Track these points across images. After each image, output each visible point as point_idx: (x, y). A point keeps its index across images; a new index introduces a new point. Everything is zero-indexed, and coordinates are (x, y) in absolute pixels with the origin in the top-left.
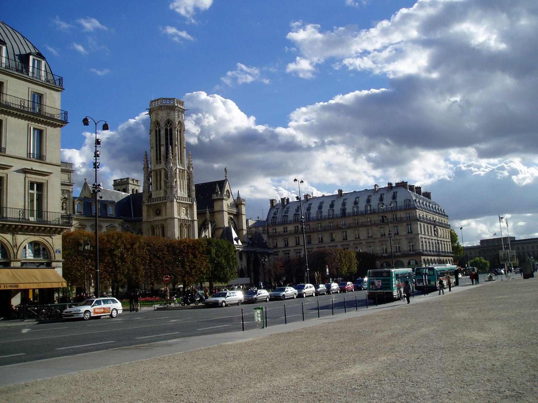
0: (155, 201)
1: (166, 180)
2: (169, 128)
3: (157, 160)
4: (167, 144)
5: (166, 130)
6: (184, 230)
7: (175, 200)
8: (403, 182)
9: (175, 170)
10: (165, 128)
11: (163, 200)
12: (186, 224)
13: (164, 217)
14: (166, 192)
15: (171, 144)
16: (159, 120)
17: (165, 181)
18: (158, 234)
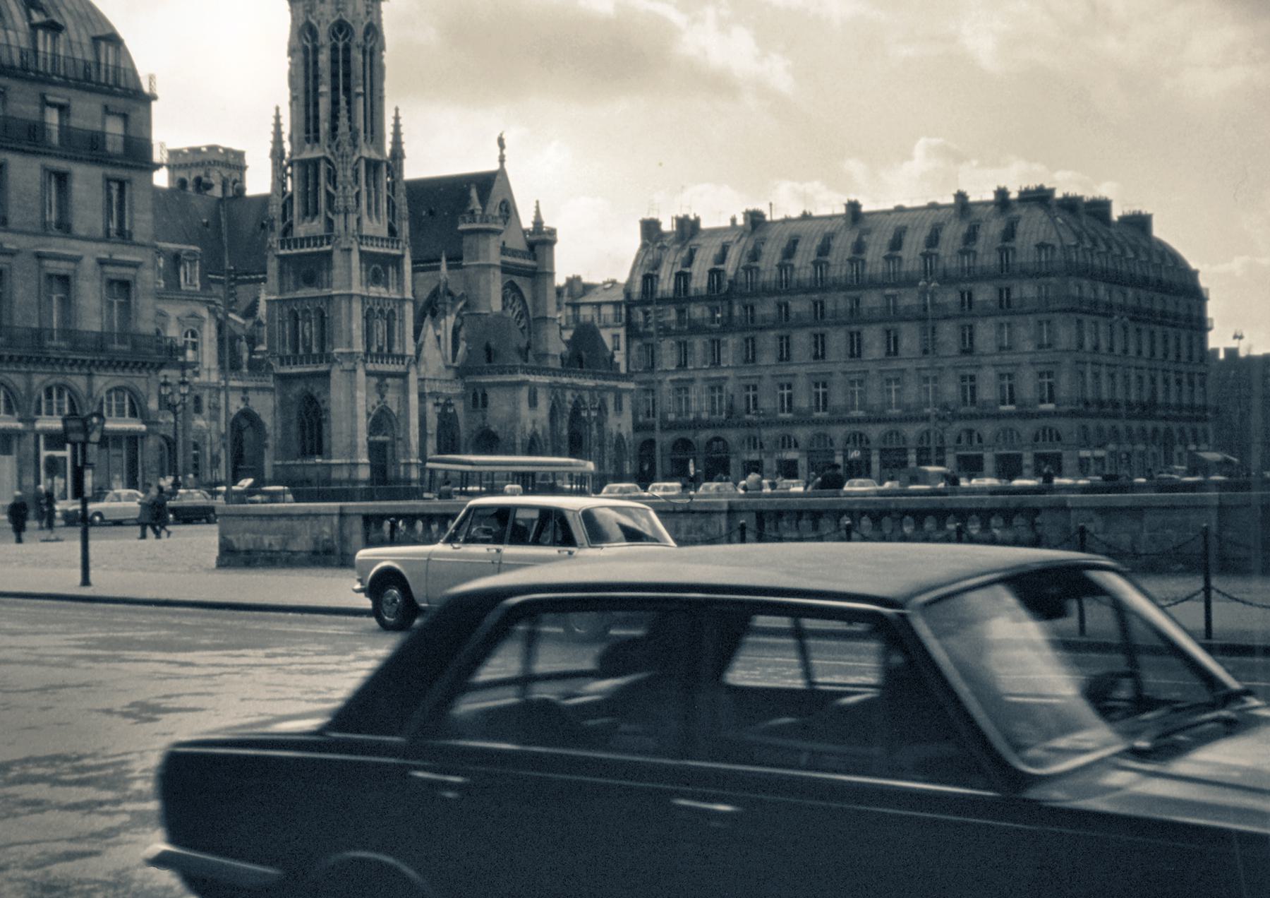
0: (302, 247)
1: (330, 189)
2: (341, 45)
3: (307, 131)
4: (335, 89)
5: (334, 49)
6: (378, 326)
7: (355, 246)
8: (1041, 189)
9: (356, 163)
10: (329, 44)
11: (322, 245)
12: (381, 311)
13: (326, 292)
14: (330, 223)
15: (347, 90)
16: (314, 22)
17: (328, 193)
18: (308, 334)
